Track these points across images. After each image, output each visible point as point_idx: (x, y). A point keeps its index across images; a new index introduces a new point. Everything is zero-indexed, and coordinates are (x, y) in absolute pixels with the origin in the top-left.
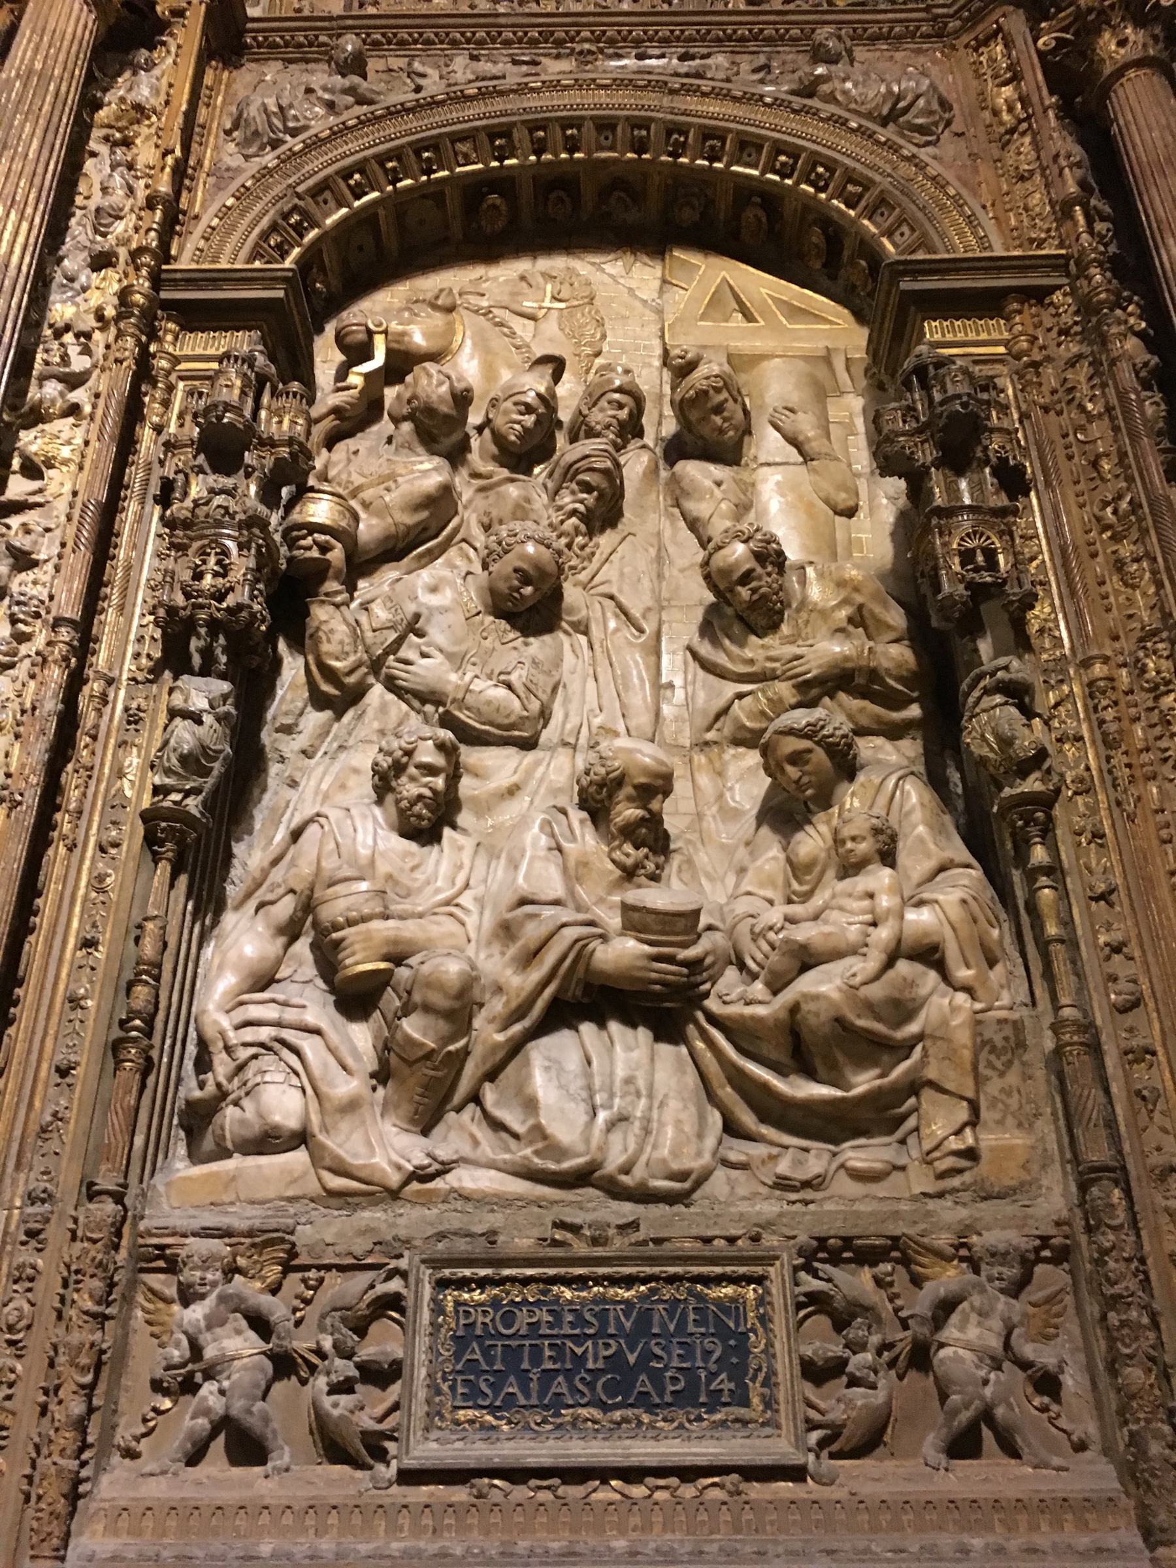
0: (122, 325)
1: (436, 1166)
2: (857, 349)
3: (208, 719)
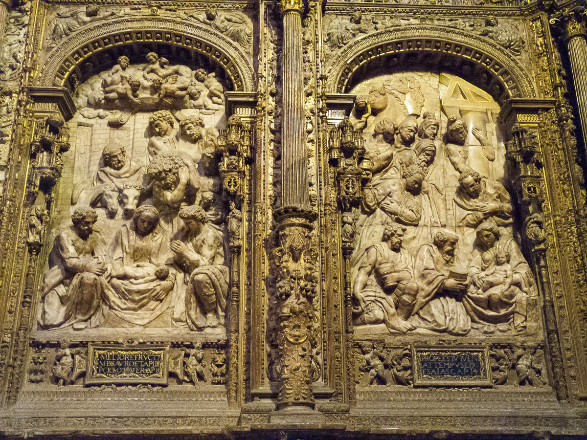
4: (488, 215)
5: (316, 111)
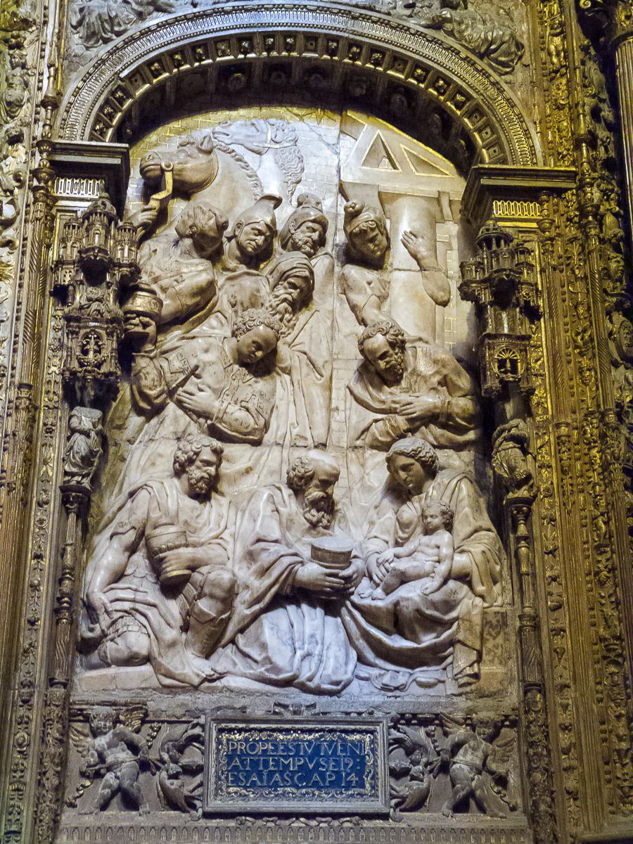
1: (216, 676)
3: (93, 434)
4: (418, 423)
5: (26, 176)
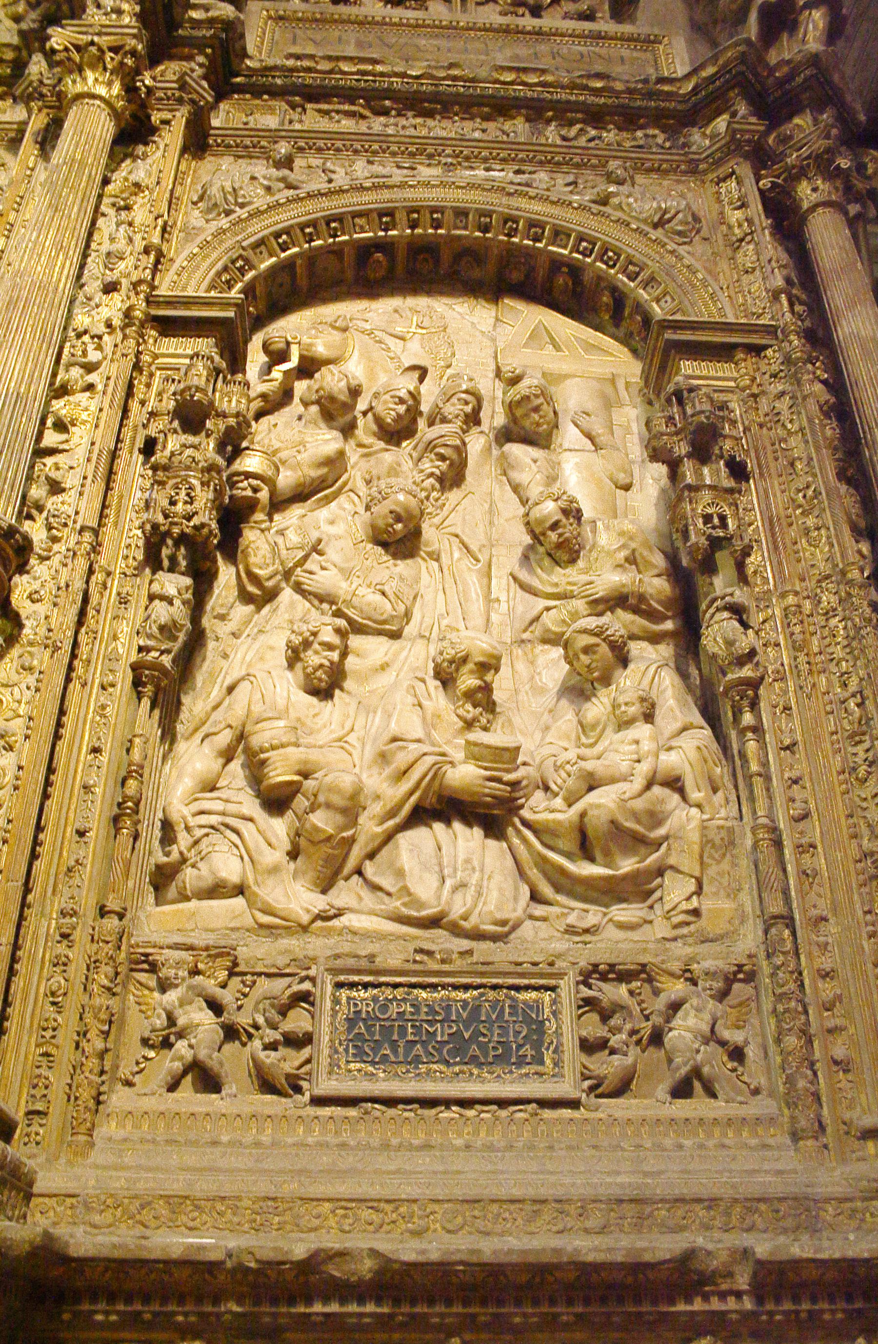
0: (128, 331)
1: (332, 912)
2: (634, 375)
3: (177, 602)
